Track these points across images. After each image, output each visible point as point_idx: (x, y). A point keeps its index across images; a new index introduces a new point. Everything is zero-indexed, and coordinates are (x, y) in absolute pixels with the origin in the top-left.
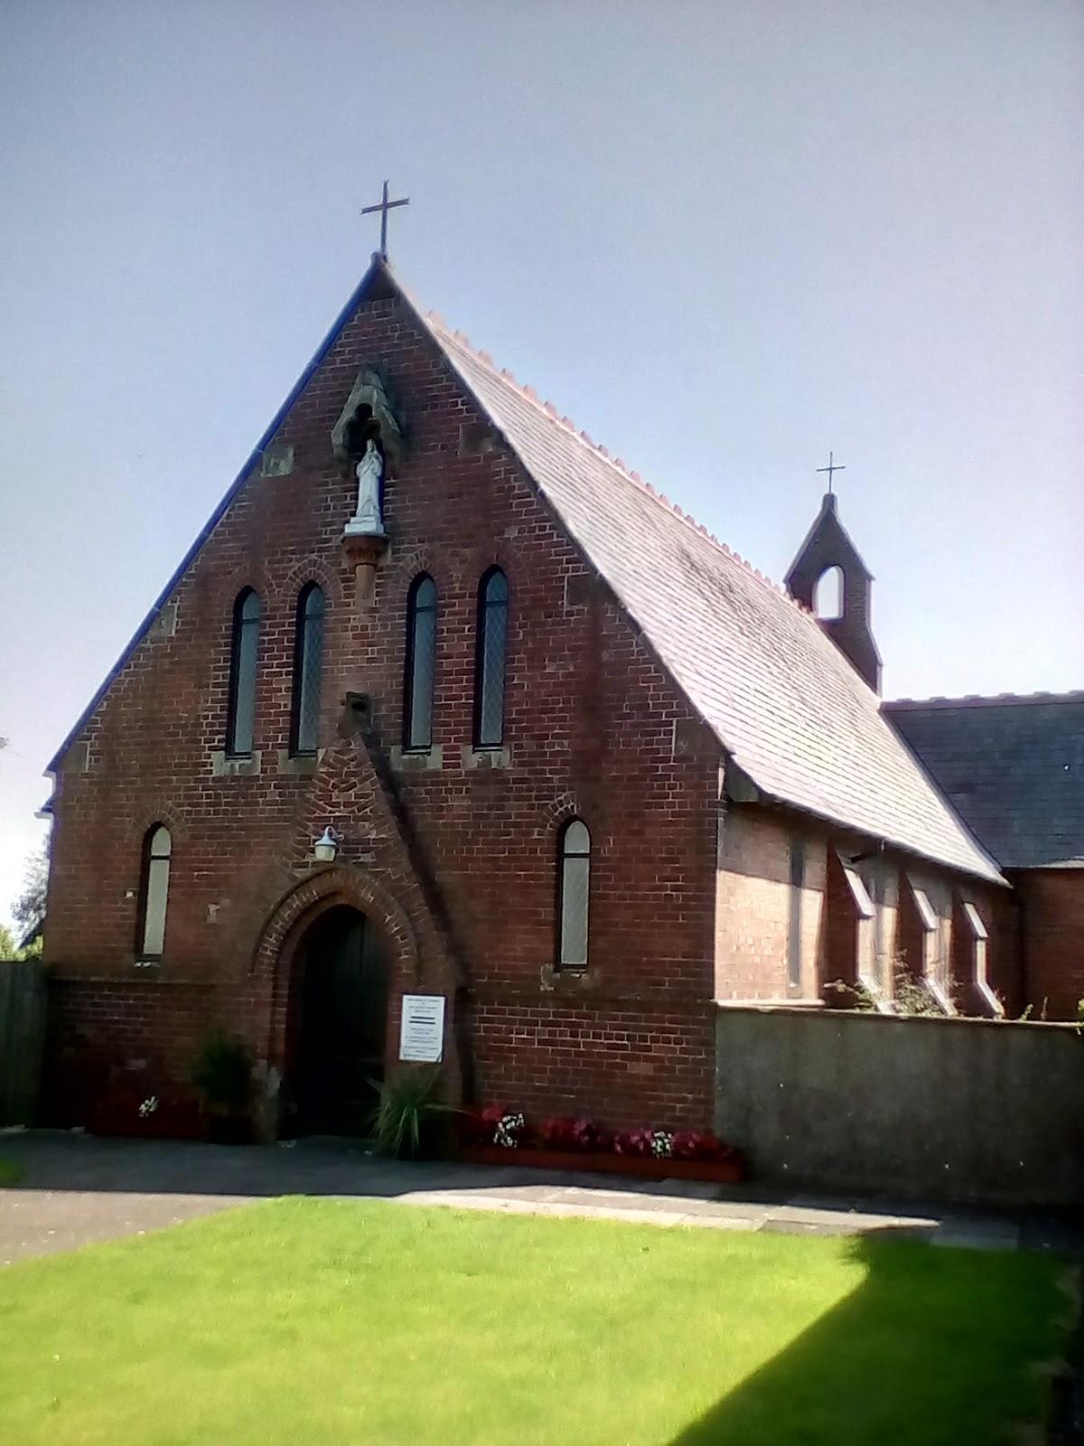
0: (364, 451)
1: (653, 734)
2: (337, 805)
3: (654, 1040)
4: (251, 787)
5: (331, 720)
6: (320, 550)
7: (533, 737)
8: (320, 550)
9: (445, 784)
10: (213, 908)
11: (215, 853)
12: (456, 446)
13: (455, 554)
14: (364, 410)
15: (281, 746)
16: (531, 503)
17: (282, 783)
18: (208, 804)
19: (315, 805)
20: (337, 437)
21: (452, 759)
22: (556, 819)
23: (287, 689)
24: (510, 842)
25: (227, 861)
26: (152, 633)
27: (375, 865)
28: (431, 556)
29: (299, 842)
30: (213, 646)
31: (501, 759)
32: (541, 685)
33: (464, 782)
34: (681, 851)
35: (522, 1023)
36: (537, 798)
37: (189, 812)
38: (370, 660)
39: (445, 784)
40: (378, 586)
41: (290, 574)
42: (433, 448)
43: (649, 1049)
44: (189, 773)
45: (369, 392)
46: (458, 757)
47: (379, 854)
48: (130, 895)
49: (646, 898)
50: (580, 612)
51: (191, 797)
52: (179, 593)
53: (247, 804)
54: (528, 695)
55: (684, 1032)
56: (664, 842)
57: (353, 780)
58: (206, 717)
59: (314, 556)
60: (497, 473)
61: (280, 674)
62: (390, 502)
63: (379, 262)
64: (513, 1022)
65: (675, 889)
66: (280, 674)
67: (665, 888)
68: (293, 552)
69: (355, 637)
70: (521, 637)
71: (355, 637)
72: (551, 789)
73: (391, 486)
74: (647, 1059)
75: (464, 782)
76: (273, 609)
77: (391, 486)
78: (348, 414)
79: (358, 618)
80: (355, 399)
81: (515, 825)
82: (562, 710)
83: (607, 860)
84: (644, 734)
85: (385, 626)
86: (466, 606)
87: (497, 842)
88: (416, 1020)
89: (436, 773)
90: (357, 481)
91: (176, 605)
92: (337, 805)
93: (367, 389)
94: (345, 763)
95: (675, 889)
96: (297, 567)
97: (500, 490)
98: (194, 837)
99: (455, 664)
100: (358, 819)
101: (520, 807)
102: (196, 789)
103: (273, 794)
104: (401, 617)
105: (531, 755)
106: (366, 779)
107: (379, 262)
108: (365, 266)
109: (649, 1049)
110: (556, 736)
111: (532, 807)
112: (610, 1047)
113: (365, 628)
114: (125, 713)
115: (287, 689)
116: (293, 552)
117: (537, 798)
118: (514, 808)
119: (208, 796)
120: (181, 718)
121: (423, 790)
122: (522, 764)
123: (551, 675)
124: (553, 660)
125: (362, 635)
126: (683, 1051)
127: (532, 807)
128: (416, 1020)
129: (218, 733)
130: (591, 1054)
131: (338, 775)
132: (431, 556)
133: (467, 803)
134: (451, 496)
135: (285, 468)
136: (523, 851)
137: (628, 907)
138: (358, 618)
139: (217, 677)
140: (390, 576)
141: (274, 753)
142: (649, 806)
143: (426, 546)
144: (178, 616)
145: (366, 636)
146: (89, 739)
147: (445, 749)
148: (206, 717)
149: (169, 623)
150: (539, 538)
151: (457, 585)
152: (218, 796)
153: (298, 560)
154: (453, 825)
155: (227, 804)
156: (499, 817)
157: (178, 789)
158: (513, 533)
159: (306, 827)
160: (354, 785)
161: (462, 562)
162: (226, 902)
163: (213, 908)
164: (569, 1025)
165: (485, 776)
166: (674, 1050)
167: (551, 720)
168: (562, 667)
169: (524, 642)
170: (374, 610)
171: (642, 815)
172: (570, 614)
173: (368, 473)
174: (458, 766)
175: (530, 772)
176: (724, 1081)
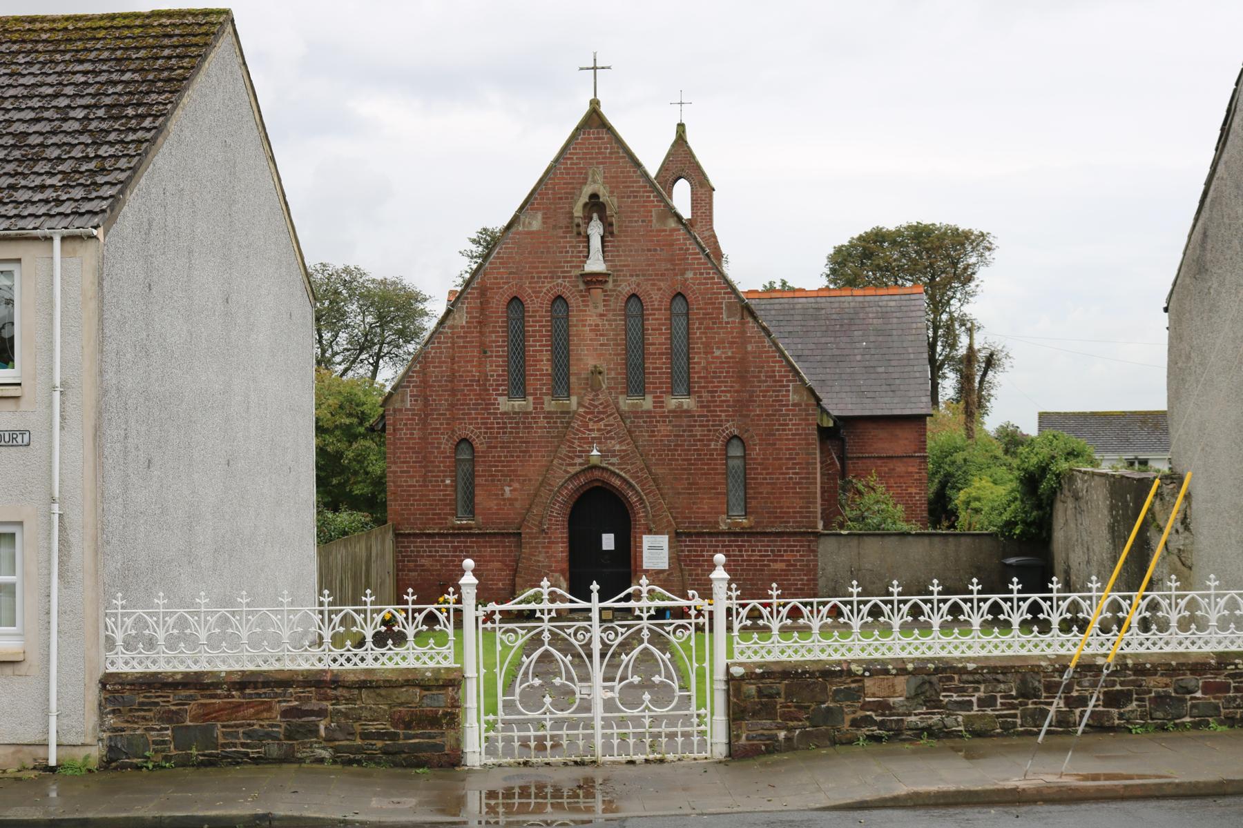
0: (591, 219)
1: (779, 391)
2: (593, 430)
3: (785, 551)
4: (527, 418)
5: (578, 379)
6: (564, 277)
7: (708, 392)
8: (564, 277)
9: (655, 417)
10: (507, 489)
11: (506, 457)
12: (651, 221)
13: (653, 285)
14: (594, 196)
15: (547, 394)
16: (700, 259)
17: (548, 416)
18: (498, 428)
19: (577, 430)
20: (578, 211)
21: (658, 403)
22: (724, 437)
23: (548, 360)
24: (698, 450)
25: (514, 461)
26: (449, 323)
27: (619, 464)
28: (638, 285)
29: (569, 452)
30: (493, 332)
31: (688, 403)
32: (713, 363)
33: (668, 417)
34: (797, 454)
35: (710, 546)
36: (713, 426)
37: (486, 433)
38: (601, 345)
39: (655, 417)
40: (604, 301)
41: (544, 290)
42: (636, 222)
43: (782, 556)
44: (482, 409)
45: (596, 185)
46: (663, 402)
47: (622, 458)
48: (448, 482)
49: (778, 479)
50: (734, 322)
51: (486, 423)
52: (466, 298)
53: (525, 428)
54: (705, 368)
55: (801, 546)
56: (787, 449)
57: (602, 416)
58: (492, 376)
59: (560, 281)
60: (679, 240)
61: (542, 351)
62: (609, 251)
63: (595, 104)
64: (705, 546)
65: (794, 473)
66: (542, 351)
67: (788, 474)
68: (546, 278)
69: (591, 330)
70: (698, 335)
71: (591, 330)
72: (721, 421)
73: (610, 241)
74: (782, 561)
75: (668, 417)
76: (533, 311)
77: (610, 241)
78: (584, 199)
79: (592, 319)
80: (588, 190)
81: (699, 440)
82: (725, 377)
83: (755, 459)
84: (774, 391)
85: (611, 325)
86: (662, 315)
87: (689, 450)
88: (651, 548)
89: (649, 412)
90: (588, 237)
91: (465, 306)
92: (593, 430)
93: (596, 186)
94: (596, 407)
95: (794, 473)
96: (548, 288)
97: (681, 249)
98: (488, 447)
99: (657, 349)
100: (606, 439)
101: (703, 431)
102: (489, 418)
103: (542, 422)
104: (621, 320)
105: (708, 401)
106: (611, 415)
107: (595, 104)
108: (586, 108)
109: (782, 556)
110: (722, 392)
111: (709, 431)
112: (761, 556)
113: (597, 325)
114: (434, 372)
115: (548, 360)
116: (546, 278)
117: (713, 426)
118: (698, 432)
119: (498, 423)
120: (474, 376)
121: (641, 421)
122: (701, 407)
123: (717, 357)
124: (718, 348)
125: (595, 329)
126: (801, 556)
127: (709, 431)
128: (651, 548)
129: (501, 385)
130: (750, 561)
131: (592, 413)
132: (638, 285)
133: (669, 428)
134: (649, 250)
135: (536, 224)
136: (706, 455)
137: (768, 484)
138: (592, 319)
139: (498, 351)
140: (611, 296)
141: (541, 398)
142: (778, 430)
143: (634, 278)
144: (467, 313)
145: (599, 330)
146: (409, 387)
147: (654, 397)
148: (492, 376)
149: (461, 318)
150: (705, 279)
151: (656, 303)
152: (505, 423)
153: (548, 283)
154: (661, 441)
155: (511, 428)
156: (691, 436)
157: (477, 419)
158: (690, 275)
159: (573, 443)
160: (603, 419)
161: (659, 289)
162: (517, 485)
163: (507, 489)
164: (736, 546)
165: (679, 413)
166: (796, 556)
167: (719, 382)
168: (723, 353)
169: (701, 338)
170: (601, 315)
171: (774, 435)
172: (727, 323)
173: (595, 231)
174: (663, 407)
175: (708, 411)
176: (823, 569)
